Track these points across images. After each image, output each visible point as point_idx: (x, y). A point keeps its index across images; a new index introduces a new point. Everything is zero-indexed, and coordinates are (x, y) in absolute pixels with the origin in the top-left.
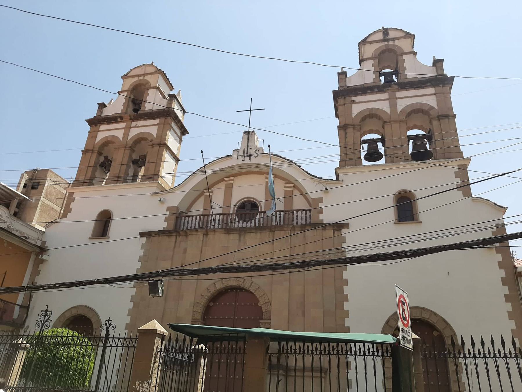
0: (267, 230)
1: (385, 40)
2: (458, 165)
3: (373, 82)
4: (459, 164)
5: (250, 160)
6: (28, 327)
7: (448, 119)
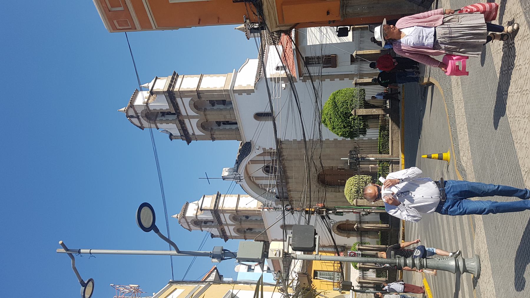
0: (285, 169)
1: (138, 117)
2: (234, 93)
3: (175, 125)
4: (233, 93)
5: (241, 177)
6: (344, 244)
7: (200, 93)
